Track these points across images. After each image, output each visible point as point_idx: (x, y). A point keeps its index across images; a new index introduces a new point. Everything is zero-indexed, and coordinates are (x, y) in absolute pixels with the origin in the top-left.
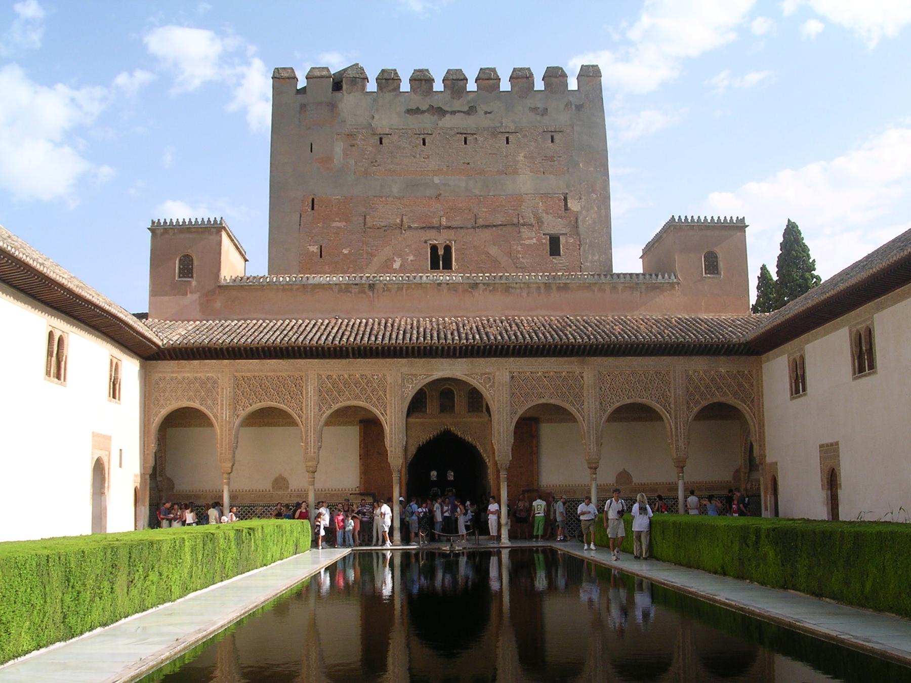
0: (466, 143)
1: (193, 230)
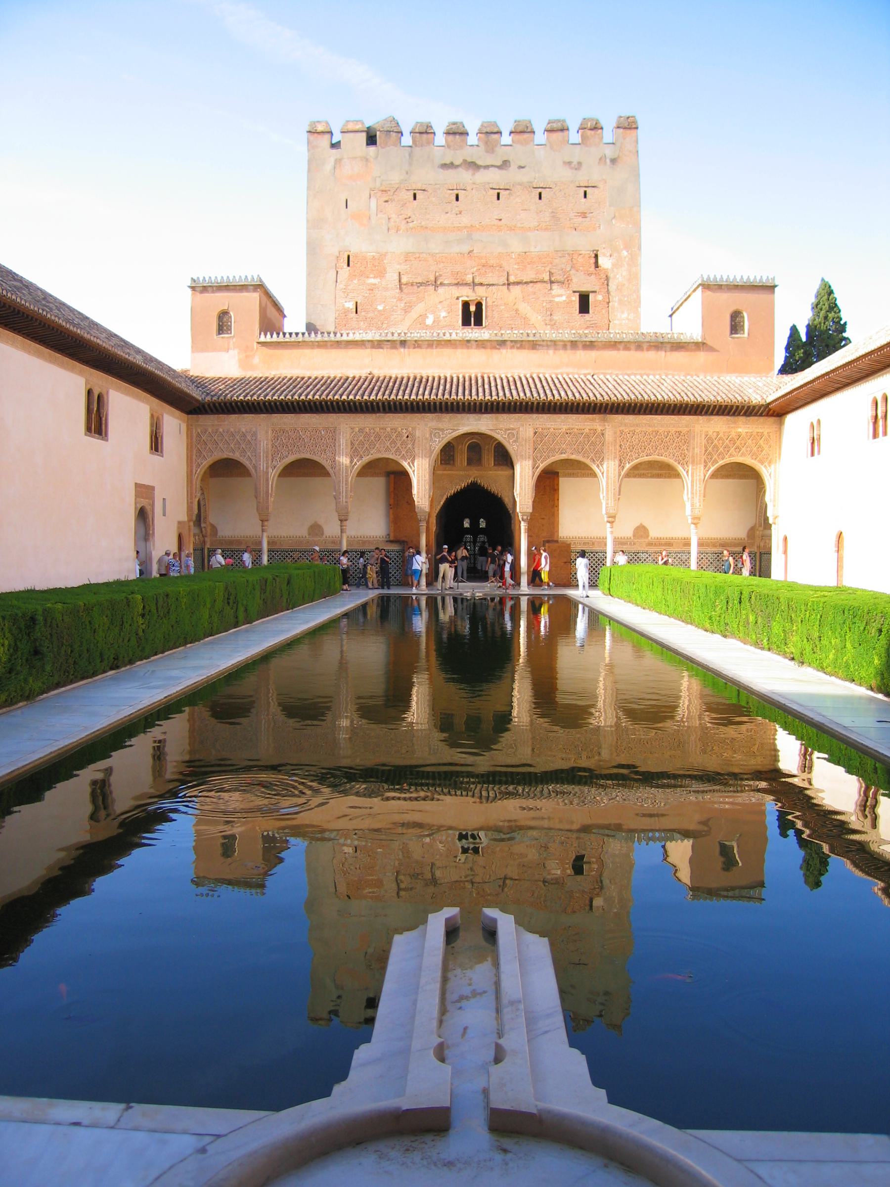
0: (498, 198)
1: (231, 287)
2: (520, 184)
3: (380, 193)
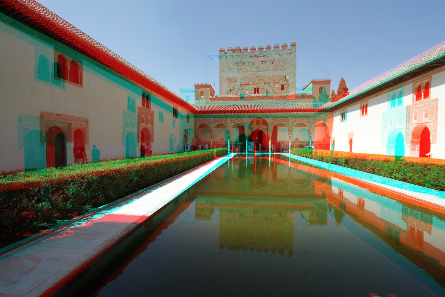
0: (263, 64)
2: (268, 60)
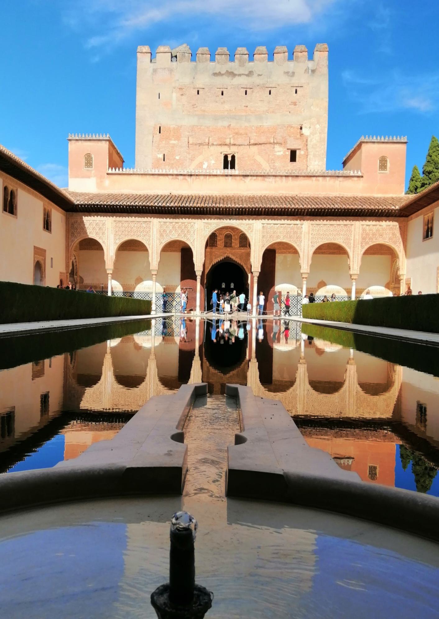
0: (246, 94)
3: (179, 89)
